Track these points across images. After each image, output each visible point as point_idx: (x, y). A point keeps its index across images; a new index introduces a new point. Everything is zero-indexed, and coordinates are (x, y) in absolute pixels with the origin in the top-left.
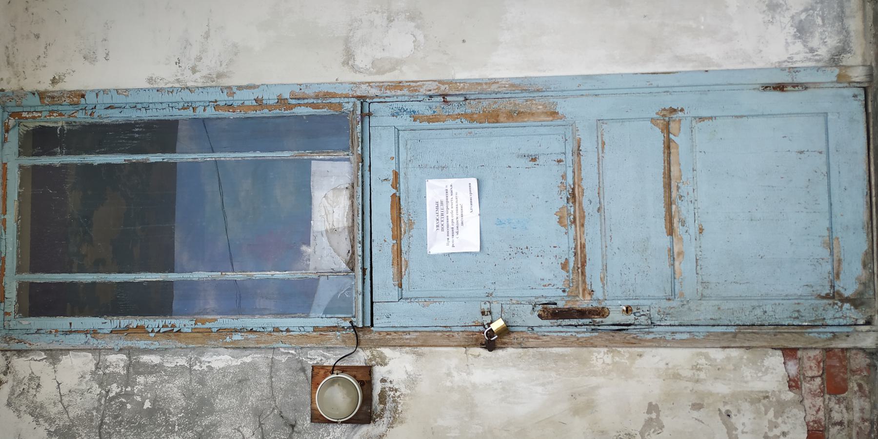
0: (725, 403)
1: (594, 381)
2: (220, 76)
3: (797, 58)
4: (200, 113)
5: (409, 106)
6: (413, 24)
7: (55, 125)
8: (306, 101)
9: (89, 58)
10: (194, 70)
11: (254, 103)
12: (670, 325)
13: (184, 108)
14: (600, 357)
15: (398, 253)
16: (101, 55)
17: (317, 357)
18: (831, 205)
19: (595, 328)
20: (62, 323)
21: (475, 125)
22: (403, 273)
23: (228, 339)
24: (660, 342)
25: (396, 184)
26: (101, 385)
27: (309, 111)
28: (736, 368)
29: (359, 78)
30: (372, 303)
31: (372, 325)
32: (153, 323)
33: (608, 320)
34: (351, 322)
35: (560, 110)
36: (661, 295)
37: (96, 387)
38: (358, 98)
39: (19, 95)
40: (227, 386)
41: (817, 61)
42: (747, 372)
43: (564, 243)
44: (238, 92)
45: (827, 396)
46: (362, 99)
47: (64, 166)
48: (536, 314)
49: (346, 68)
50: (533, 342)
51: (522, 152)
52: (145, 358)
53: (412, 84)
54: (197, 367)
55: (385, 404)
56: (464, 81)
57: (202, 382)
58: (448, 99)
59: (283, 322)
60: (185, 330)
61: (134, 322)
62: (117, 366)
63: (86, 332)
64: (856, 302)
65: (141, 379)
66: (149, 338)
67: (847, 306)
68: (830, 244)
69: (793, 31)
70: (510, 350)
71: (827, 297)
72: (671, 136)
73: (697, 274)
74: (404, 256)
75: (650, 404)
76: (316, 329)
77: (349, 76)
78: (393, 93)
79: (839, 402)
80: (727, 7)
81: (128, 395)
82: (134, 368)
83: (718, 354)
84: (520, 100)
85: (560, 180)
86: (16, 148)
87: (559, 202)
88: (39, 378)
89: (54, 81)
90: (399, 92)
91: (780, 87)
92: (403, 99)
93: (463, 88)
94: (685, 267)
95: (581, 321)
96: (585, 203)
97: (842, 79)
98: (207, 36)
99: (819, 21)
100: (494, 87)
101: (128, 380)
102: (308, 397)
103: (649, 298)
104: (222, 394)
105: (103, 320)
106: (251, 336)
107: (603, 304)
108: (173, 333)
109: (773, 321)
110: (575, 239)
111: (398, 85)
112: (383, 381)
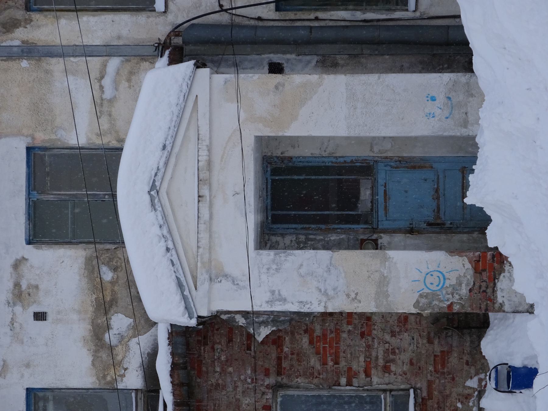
2: (333, 153)
4: (327, 164)
5: (389, 163)
13: (323, 163)
14: (443, 237)
15: (386, 207)
17: (362, 237)
21: (409, 169)
23: (336, 231)
24: (460, 233)
25: (385, 187)
27: (360, 164)
31: (378, 227)
33: (445, 226)
35: (434, 166)
39: (271, 157)
43: (434, 204)
44: (339, 159)
46: (376, 161)
52: (311, 237)
56: (405, 157)
57: (328, 243)
61: (307, 226)
62: (303, 238)
65: (310, 242)
72: (465, 175)
74: (387, 208)
77: (372, 154)
88: (279, 242)
89: (282, 153)
90: (387, 160)
95: (438, 227)
96: (440, 193)
101: (305, 243)
105: (298, 225)
110: (437, 203)
111: (386, 158)
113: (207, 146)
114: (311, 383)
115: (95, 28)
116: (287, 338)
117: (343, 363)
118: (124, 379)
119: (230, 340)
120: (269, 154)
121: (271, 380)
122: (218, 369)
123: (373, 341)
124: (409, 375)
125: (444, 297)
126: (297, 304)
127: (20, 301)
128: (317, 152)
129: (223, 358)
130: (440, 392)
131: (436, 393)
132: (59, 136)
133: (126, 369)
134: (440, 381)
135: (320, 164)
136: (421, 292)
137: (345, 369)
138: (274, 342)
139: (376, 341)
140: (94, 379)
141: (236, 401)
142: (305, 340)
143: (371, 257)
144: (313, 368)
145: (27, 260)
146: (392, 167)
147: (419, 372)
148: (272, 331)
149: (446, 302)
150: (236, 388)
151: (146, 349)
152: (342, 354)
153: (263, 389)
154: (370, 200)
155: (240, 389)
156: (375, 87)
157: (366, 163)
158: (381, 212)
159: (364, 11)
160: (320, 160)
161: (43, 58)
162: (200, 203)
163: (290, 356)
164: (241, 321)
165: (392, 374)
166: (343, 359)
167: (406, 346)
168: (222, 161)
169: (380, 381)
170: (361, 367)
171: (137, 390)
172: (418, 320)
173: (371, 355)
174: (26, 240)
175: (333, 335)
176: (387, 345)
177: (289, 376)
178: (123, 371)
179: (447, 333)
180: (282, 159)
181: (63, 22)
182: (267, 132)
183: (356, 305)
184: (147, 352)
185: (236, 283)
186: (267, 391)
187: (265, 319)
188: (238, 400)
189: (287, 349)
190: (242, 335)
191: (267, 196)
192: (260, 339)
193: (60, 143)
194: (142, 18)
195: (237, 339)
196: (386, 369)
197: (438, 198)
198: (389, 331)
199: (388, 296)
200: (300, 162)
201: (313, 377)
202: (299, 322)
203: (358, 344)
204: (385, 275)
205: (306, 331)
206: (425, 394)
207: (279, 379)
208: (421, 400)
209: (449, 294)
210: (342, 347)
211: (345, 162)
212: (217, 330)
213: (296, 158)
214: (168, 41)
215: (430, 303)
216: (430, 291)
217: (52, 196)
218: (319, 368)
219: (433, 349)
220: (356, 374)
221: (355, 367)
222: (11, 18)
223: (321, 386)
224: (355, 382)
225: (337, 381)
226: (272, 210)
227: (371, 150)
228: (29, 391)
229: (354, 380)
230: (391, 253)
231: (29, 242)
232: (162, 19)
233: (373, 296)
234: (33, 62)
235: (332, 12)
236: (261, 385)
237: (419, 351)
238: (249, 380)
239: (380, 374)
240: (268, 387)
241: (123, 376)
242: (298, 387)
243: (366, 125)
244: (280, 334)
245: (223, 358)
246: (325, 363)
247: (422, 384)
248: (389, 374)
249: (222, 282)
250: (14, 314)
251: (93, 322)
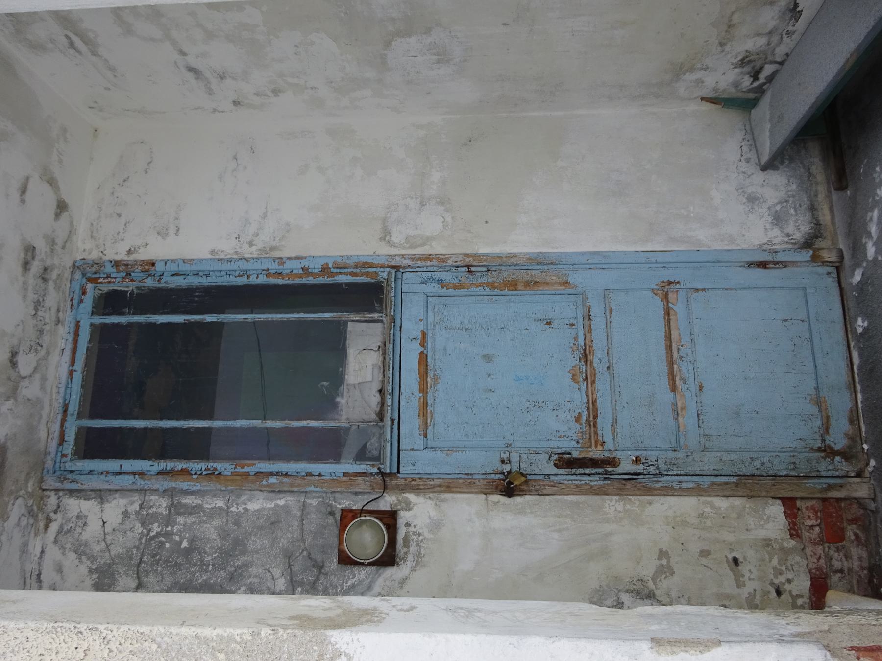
0: (732, 550)
1: (607, 528)
2: (273, 249)
3: (775, 241)
4: (254, 280)
5: (437, 275)
6: (443, 208)
7: (126, 289)
8: (346, 270)
9: (163, 233)
10: (251, 244)
11: (301, 272)
12: (677, 475)
13: (240, 276)
14: (612, 505)
15: (424, 406)
16: (172, 230)
17: (345, 503)
18: (816, 367)
19: (607, 476)
20: (113, 465)
21: (496, 292)
22: (429, 424)
23: (264, 482)
24: (668, 491)
25: (423, 344)
26: (143, 524)
28: (740, 516)
29: (393, 251)
30: (399, 451)
31: (399, 472)
32: (196, 466)
33: (620, 469)
34: (379, 468)
35: (572, 282)
36: (667, 446)
37: (139, 528)
38: (393, 267)
39: (98, 264)
40: (261, 528)
41: (792, 244)
42: (751, 521)
43: (578, 398)
44: (288, 262)
45: (826, 545)
46: (396, 268)
47: (130, 325)
48: (552, 463)
49: (383, 243)
50: (548, 490)
51: (538, 316)
52: (188, 500)
53: (440, 256)
54: (233, 509)
55: (408, 548)
56: (487, 255)
57: (237, 523)
58: (473, 269)
59: (316, 467)
60: (226, 473)
61: (179, 465)
62: (160, 506)
63: (134, 474)
64: (847, 455)
65: (181, 520)
66: (192, 480)
67: (838, 458)
68: (818, 402)
69: (770, 219)
70: (528, 498)
71: (819, 450)
72: (670, 304)
73: (699, 427)
74: (429, 409)
75: (661, 551)
76: (346, 474)
77: (385, 250)
78: (424, 264)
79: (838, 550)
80: (712, 199)
81: (168, 535)
82: (176, 509)
83: (722, 503)
84: (536, 273)
85: (572, 341)
86: (89, 309)
87: (573, 361)
88: (86, 517)
89: (129, 252)
90: (429, 263)
91: (763, 265)
92: (432, 269)
93: (486, 260)
94: (688, 421)
95: (594, 471)
97: (816, 258)
98: (264, 216)
99: (792, 211)
100: (513, 260)
101: (168, 520)
102: (336, 540)
103: (657, 449)
104: (256, 535)
105: (151, 463)
106: (285, 480)
107: (614, 455)
108: (214, 475)
109: (771, 472)
111: (429, 257)
112: (408, 525)
120: (94, 255)
128: (227, 247)
135: (232, 278)
146: (442, 284)
154: (376, 386)
158: (410, 423)
191: (71, 373)
197: (589, 380)
213: (166, 263)
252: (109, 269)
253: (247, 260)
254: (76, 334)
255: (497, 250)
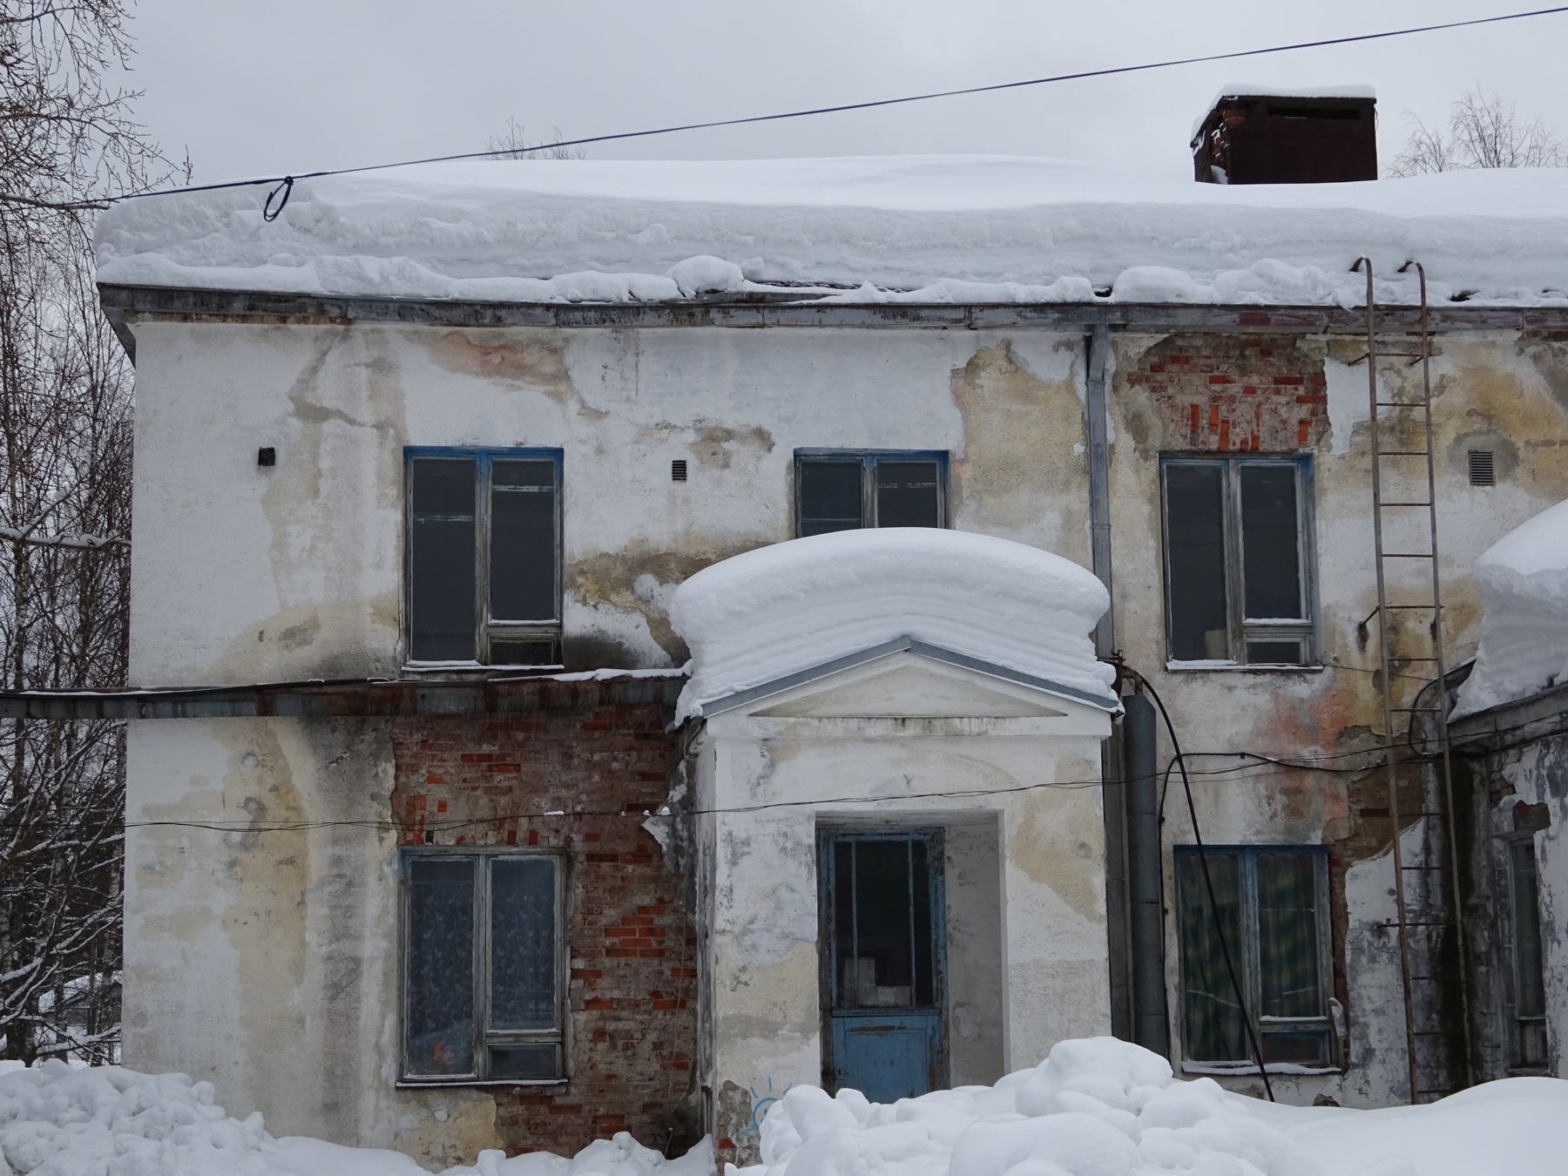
2: (951, 941)
4: (933, 932)
16: (962, 882)
20: (832, 865)
25: (899, 1028)
29: (950, 1010)
39: (942, 841)
46: (941, 1012)
47: (907, 864)
61: (833, 902)
77: (951, 1004)
89: (949, 858)
108: (829, 919)
111: (947, 1029)
113: (986, 732)
114: (576, 909)
115: (1137, 559)
116: (648, 871)
117: (607, 962)
118: (579, 605)
119: (644, 776)
120: (947, 837)
121: (578, 843)
122: (596, 757)
123: (645, 1013)
124: (590, 1073)
125: (743, 1133)
126: (728, 884)
127: (703, 440)
128: (952, 915)
129: (615, 765)
130: (563, 1126)
131: (561, 1119)
132: (967, 502)
133: (595, 607)
134: (582, 1125)
136: (751, 1094)
137: (599, 967)
138: (641, 848)
139: (646, 1017)
140: (579, 557)
141: (545, 787)
142: (646, 900)
143: (809, 1008)
144: (601, 914)
145: (770, 450)
146: (932, 1037)
147: (596, 1091)
148: (661, 847)
149: (735, 1136)
150: (568, 786)
151: (628, 640)
152: (623, 960)
153: (565, 831)
154: (877, 1003)
155: (564, 793)
156: (1089, 1010)
157: (937, 996)
158: (857, 1022)
159: (1178, 988)
160: (941, 922)
161: (1088, 477)
162: (893, 721)
163: (620, 875)
164: (677, 793)
165: (592, 1045)
166: (616, 963)
167: (639, 1068)
168: (961, 756)
169: (580, 1025)
170: (603, 994)
171: (560, 626)
172: (682, 1087)
173: (623, 1009)
174: (801, 449)
175: (654, 945)
176: (640, 1036)
177: (586, 873)
178: (592, 603)
179: (661, 1136)
180: (940, 857)
181: (1146, 509)
182: (1009, 832)
183: (728, 982)
184: (624, 641)
185: (761, 781)
186: (562, 838)
187: (681, 833)
188: (546, 790)
189: (630, 871)
190: (652, 794)
191: (881, 834)
192: (647, 825)
193: (956, 502)
194: (1155, 633)
195: (647, 788)
196: (599, 1035)
198: (662, 1039)
199: (744, 1037)
200: (936, 887)
201: (583, 913)
202: (676, 889)
203: (641, 987)
204: (779, 1032)
205: (661, 900)
206: (558, 1101)
207: (582, 858)
208: (548, 1094)
209: (748, 1141)
210: (634, 961)
211: (938, 961)
212: (662, 756)
214: (1128, 673)
215: (733, 1110)
216: (753, 1108)
217: (870, 491)
218: (600, 924)
219: (633, 1114)
220: (591, 986)
221: (604, 983)
222: (1148, 428)
223: (570, 927)
224: (581, 982)
225: (579, 954)
226: (858, 843)
227: (960, 1005)
228: (559, 453)
229: (581, 981)
230: (816, 1041)
231: (795, 451)
232: (1156, 664)
233: (744, 1012)
234: (1082, 463)
235: (1176, 938)
236: (571, 830)
237: (631, 1089)
238: (579, 808)
239: (592, 1025)
240: (569, 840)
241: (584, 602)
242: (567, 888)
243: (1026, 995)
244: (655, 858)
245: (615, 765)
246: (608, 932)
247: (576, 1095)
248: (591, 1041)
249: (764, 760)
250: (682, 429)
251: (670, 554)
252: (939, 848)
253: (945, 928)
254: (901, 834)
255: (952, 1067)
